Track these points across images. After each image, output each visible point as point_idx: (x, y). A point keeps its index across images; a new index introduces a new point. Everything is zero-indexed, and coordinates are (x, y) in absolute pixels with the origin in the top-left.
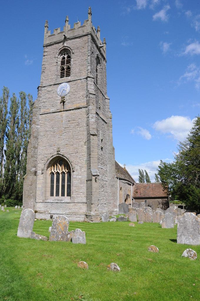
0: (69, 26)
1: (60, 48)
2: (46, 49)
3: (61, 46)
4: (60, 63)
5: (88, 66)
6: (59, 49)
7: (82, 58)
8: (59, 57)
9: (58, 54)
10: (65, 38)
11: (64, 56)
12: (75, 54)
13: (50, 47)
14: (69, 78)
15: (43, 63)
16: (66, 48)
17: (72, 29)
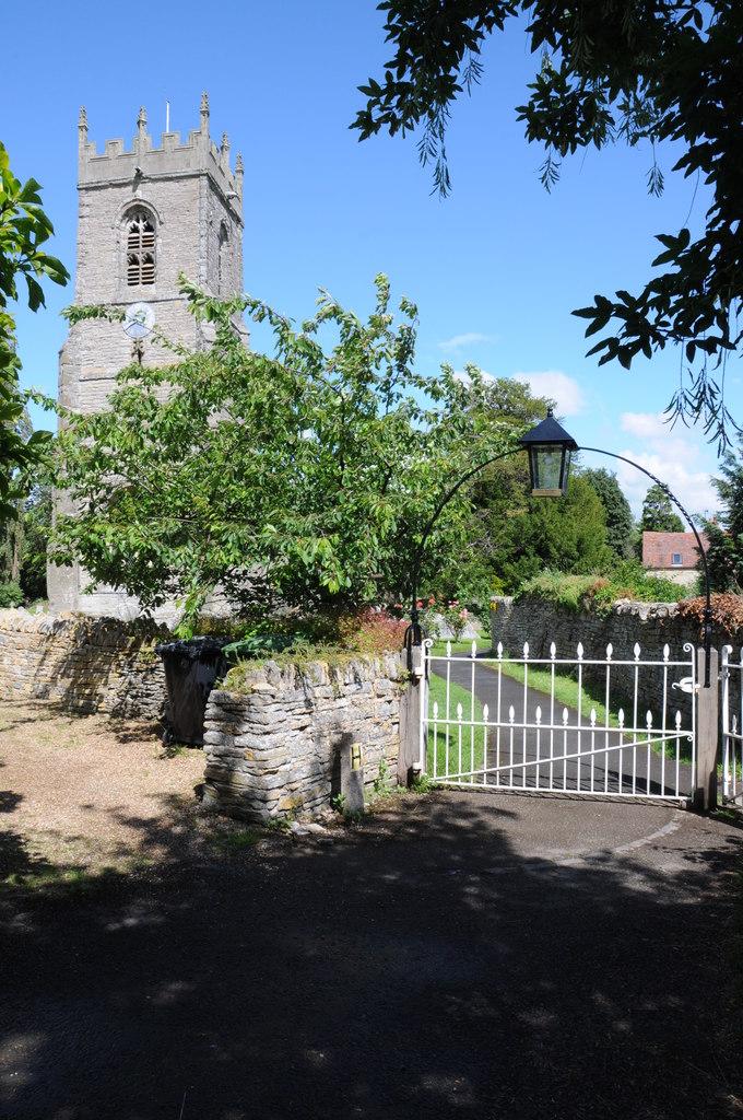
0: (149, 139)
1: (125, 201)
2: (89, 198)
3: (126, 196)
4: (125, 242)
5: (200, 264)
6: (122, 204)
7: (185, 240)
8: (123, 225)
9: (120, 217)
10: (139, 175)
11: (137, 224)
12: (168, 226)
13: (98, 192)
14: (152, 290)
15: (79, 239)
16: (143, 204)
17: (158, 153)
